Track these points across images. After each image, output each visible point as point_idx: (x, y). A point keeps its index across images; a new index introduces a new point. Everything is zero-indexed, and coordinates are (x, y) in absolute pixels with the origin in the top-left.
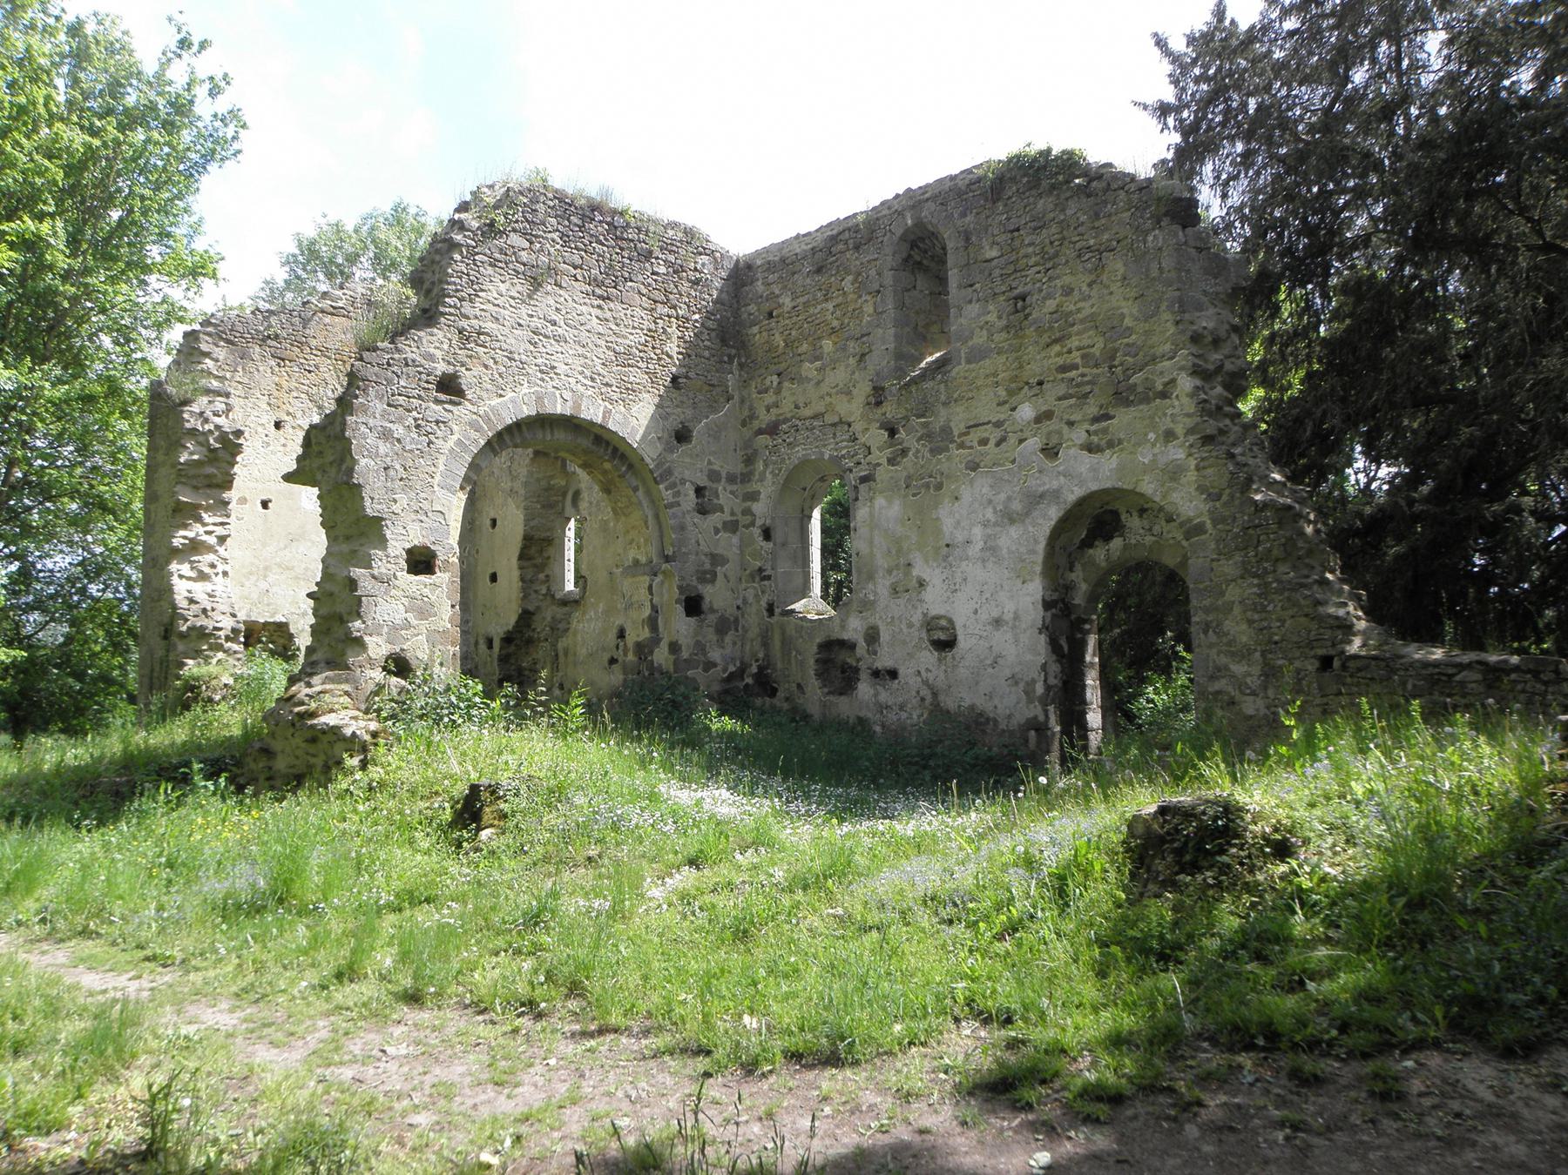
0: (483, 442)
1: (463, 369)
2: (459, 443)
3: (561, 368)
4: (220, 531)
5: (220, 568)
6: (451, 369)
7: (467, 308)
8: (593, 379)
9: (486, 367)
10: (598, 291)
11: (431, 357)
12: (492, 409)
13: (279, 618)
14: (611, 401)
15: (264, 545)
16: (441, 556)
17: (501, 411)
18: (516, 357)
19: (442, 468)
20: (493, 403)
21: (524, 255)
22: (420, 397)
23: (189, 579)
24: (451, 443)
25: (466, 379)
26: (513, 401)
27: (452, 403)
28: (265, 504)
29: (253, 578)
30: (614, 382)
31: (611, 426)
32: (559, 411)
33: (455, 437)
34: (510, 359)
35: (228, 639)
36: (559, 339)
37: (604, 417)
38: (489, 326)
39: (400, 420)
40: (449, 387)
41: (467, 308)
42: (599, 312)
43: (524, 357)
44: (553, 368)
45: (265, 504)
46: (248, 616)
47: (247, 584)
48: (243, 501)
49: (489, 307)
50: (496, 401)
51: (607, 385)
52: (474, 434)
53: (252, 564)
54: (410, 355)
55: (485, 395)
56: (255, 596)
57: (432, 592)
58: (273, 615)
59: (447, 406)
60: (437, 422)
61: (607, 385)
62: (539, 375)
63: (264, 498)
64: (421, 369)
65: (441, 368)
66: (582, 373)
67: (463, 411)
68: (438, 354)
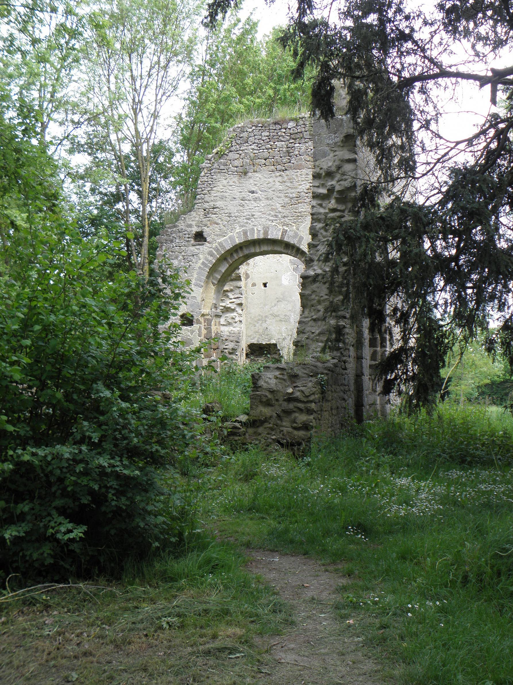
0: (214, 261)
1: (206, 228)
2: (203, 263)
3: (257, 214)
4: (238, 301)
5: (237, 319)
6: (199, 230)
7: (207, 198)
8: (276, 216)
9: (217, 224)
10: (279, 167)
11: (190, 226)
12: (220, 244)
13: (273, 342)
14: (287, 225)
15: (265, 305)
16: (195, 318)
17: (224, 244)
18: (233, 215)
19: (195, 276)
20: (219, 241)
21: (236, 163)
22: (185, 246)
23: (224, 325)
24: (199, 264)
25: (207, 231)
26: (230, 238)
27: (199, 245)
28: (265, 285)
29: (260, 322)
30: (290, 215)
31: (285, 239)
32: (256, 237)
33: (201, 261)
34: (229, 217)
35: (230, 353)
36: (255, 199)
37: (282, 235)
38: (219, 204)
39: (176, 258)
40: (200, 237)
41: (207, 198)
42: (280, 179)
43: (237, 214)
44: (253, 215)
45: (265, 285)
46: (258, 341)
47: (257, 325)
48: (254, 285)
49: (218, 194)
50: (222, 239)
51: (284, 217)
52: (210, 258)
53: (259, 315)
54: (180, 227)
55: (216, 237)
56: (261, 331)
57: (192, 334)
58: (269, 340)
59: (198, 247)
60: (193, 255)
61: (284, 217)
62: (245, 221)
63: (264, 282)
64: (186, 232)
65: (195, 229)
66: (269, 214)
67: (205, 248)
68: (194, 223)
